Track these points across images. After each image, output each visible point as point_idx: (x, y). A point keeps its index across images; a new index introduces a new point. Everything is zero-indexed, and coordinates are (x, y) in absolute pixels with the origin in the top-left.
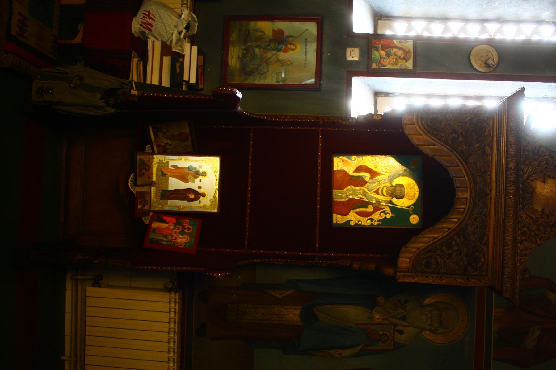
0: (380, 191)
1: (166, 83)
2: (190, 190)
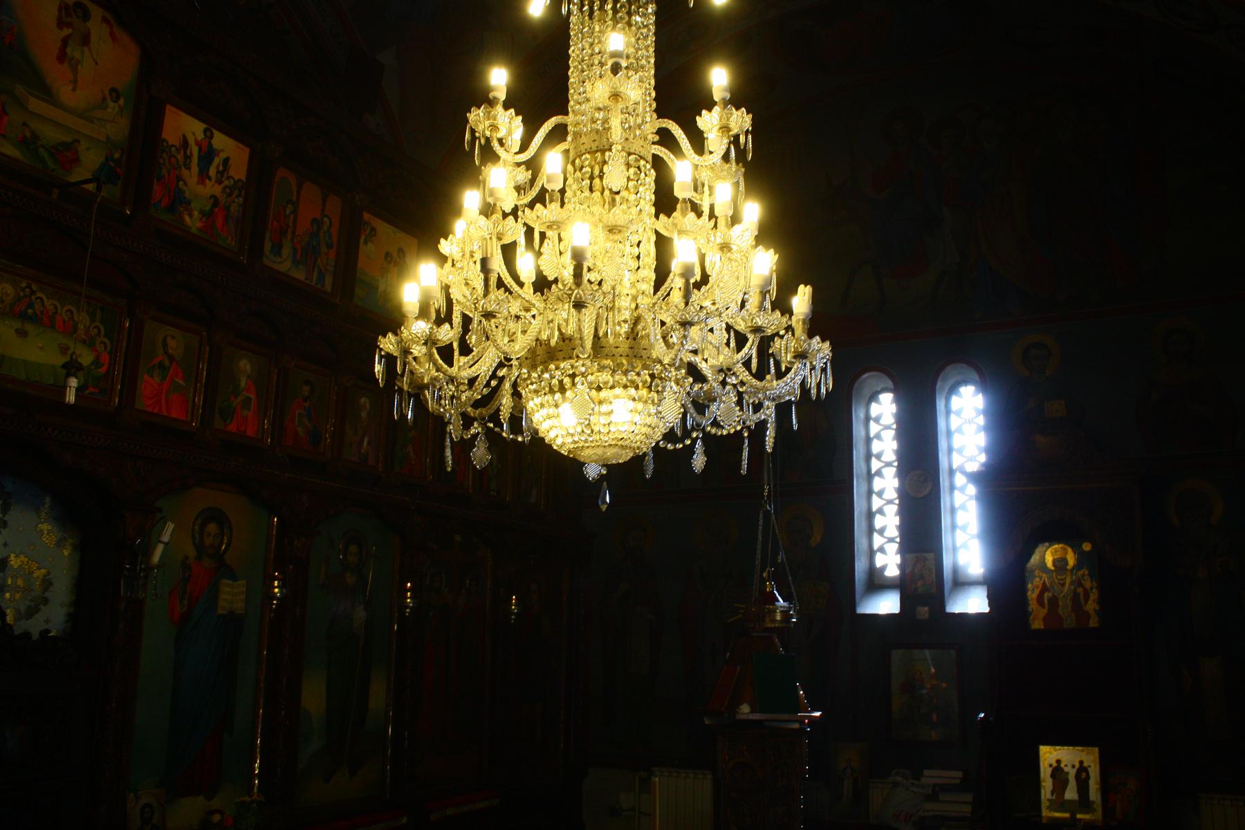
1: (969, 797)
2: (1078, 776)
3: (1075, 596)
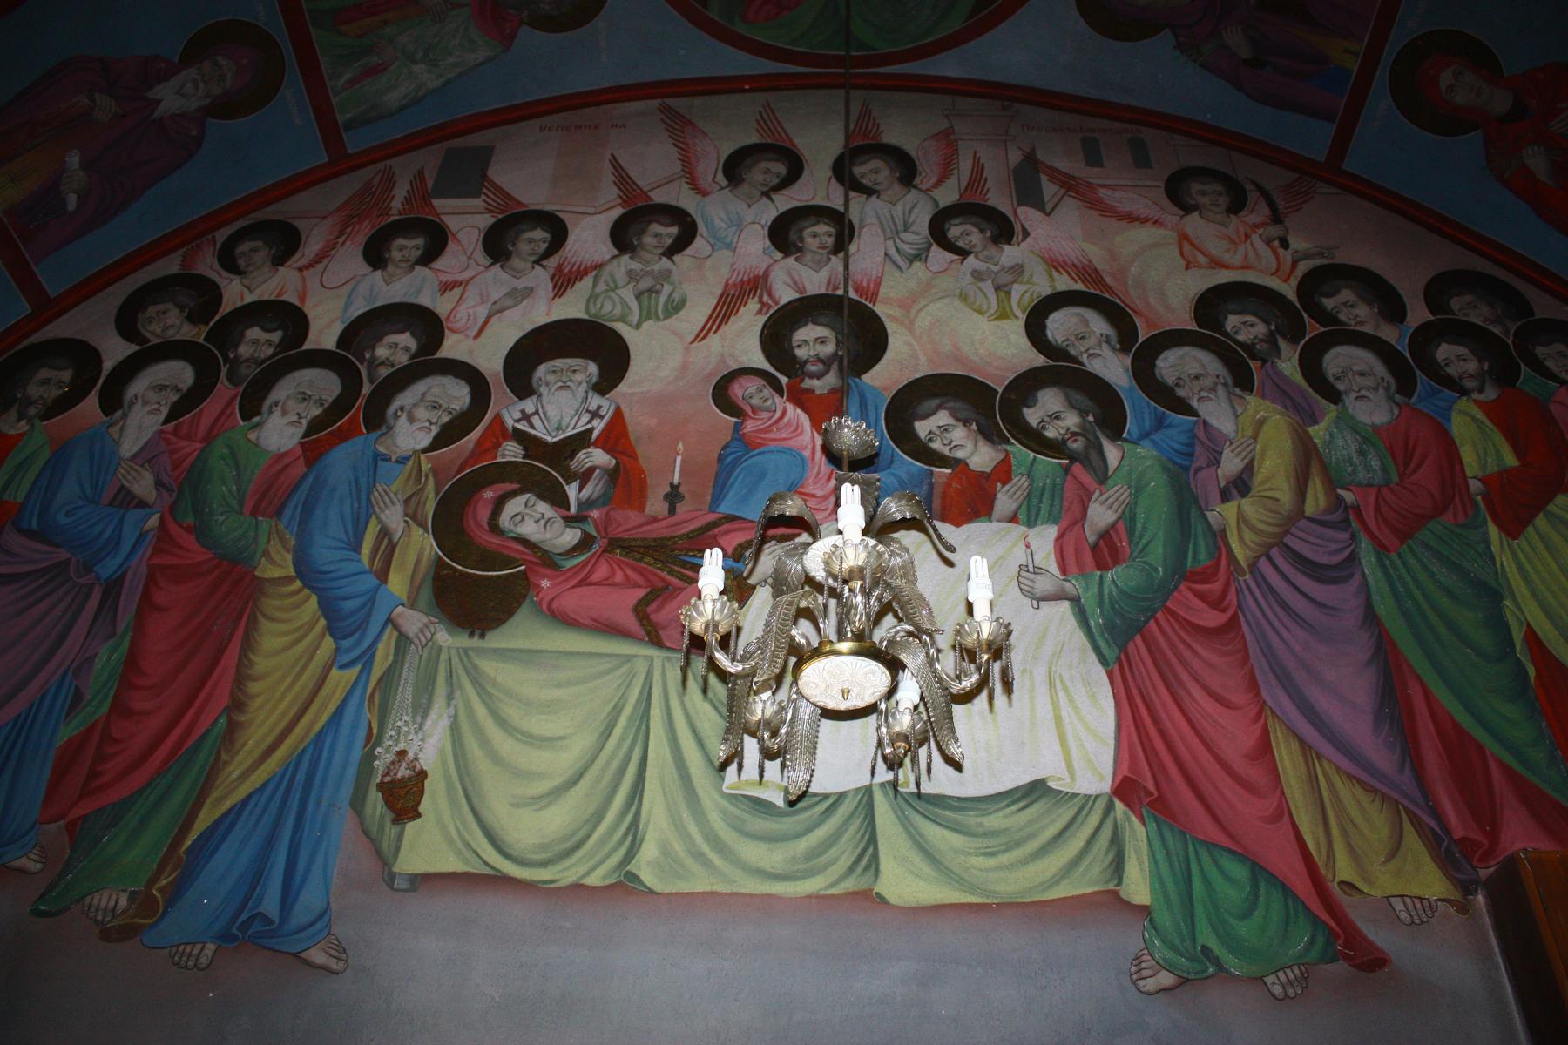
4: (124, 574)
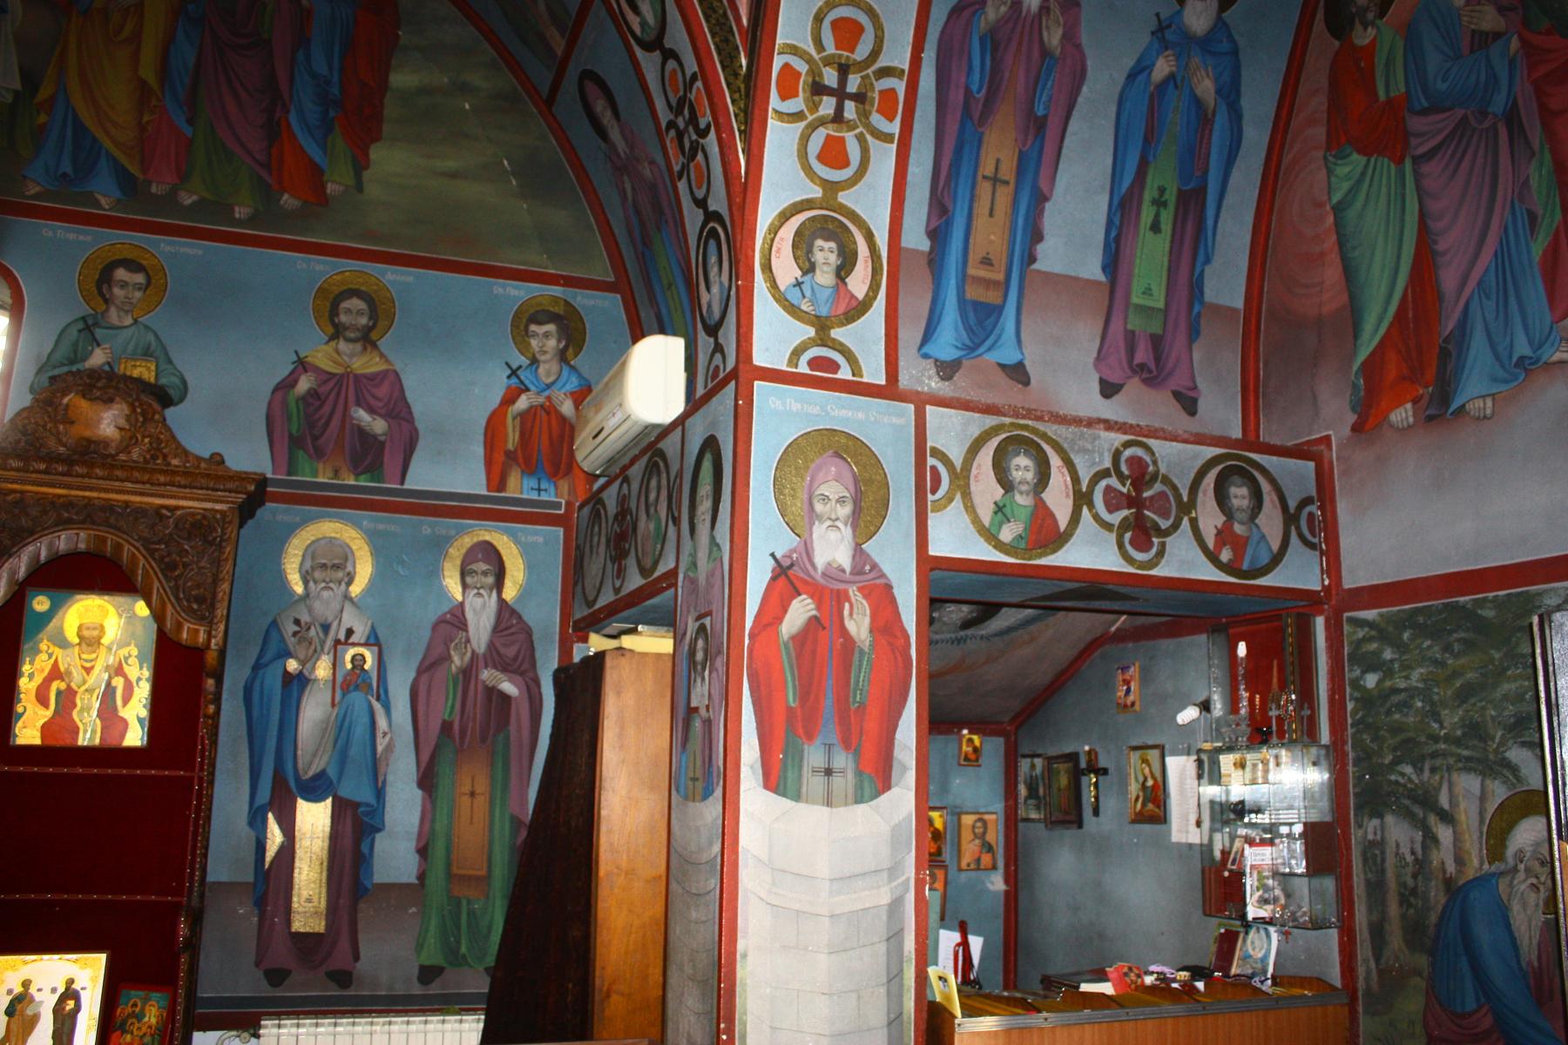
0: (88, 665)
3: (109, 690)
4: (1515, 103)
